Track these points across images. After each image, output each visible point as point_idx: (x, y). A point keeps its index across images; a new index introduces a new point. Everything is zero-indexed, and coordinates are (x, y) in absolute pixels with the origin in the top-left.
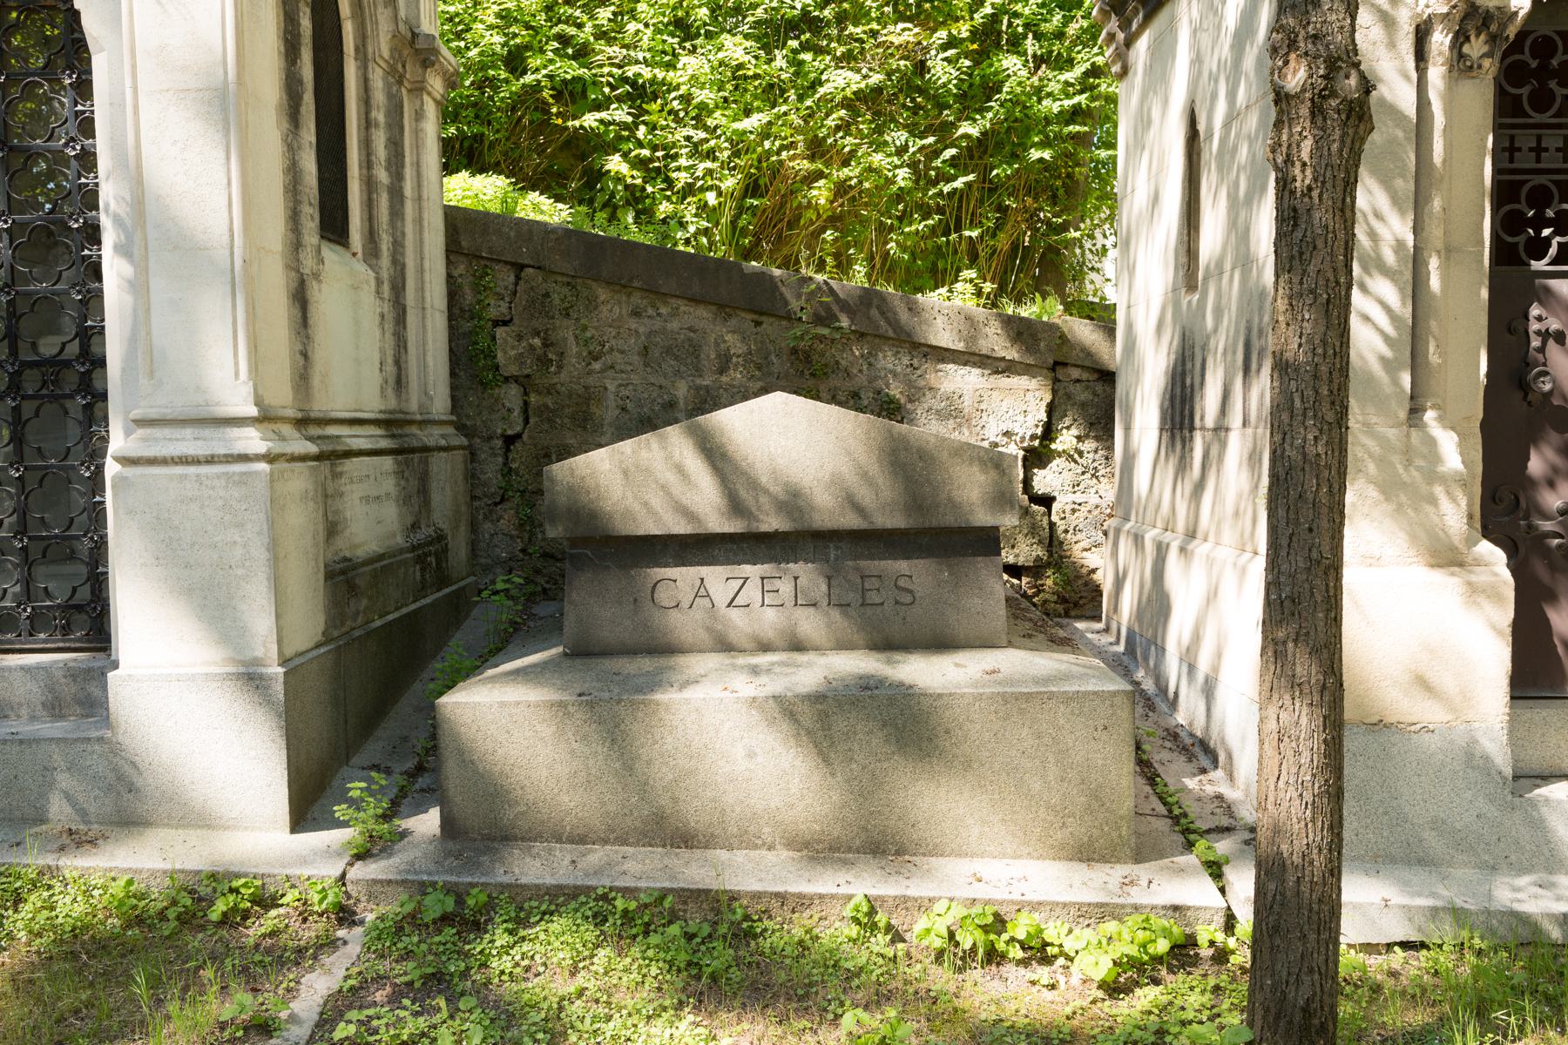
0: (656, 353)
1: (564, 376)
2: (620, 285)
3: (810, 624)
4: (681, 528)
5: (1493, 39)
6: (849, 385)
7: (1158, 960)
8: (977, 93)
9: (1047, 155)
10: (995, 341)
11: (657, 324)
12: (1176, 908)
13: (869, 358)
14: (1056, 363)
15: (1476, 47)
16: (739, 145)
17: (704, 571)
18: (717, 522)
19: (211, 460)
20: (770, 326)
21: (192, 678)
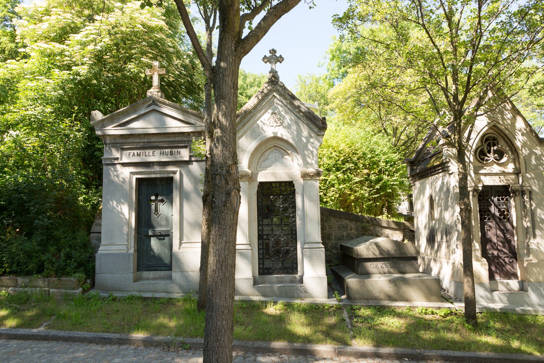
0: (340, 228)
1: (326, 231)
2: (335, 217)
3: (392, 270)
4: (375, 257)
5: (477, 192)
6: (371, 233)
7: (448, 314)
8: (379, 180)
9: (390, 191)
10: (393, 226)
11: (341, 223)
12: (449, 308)
13: (374, 228)
14: (405, 229)
15: (475, 193)
16: (340, 190)
17: (377, 263)
18: (379, 256)
19: (317, 248)
20: (359, 223)
21: (315, 277)
